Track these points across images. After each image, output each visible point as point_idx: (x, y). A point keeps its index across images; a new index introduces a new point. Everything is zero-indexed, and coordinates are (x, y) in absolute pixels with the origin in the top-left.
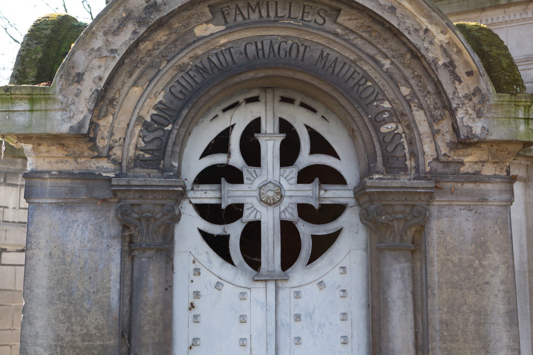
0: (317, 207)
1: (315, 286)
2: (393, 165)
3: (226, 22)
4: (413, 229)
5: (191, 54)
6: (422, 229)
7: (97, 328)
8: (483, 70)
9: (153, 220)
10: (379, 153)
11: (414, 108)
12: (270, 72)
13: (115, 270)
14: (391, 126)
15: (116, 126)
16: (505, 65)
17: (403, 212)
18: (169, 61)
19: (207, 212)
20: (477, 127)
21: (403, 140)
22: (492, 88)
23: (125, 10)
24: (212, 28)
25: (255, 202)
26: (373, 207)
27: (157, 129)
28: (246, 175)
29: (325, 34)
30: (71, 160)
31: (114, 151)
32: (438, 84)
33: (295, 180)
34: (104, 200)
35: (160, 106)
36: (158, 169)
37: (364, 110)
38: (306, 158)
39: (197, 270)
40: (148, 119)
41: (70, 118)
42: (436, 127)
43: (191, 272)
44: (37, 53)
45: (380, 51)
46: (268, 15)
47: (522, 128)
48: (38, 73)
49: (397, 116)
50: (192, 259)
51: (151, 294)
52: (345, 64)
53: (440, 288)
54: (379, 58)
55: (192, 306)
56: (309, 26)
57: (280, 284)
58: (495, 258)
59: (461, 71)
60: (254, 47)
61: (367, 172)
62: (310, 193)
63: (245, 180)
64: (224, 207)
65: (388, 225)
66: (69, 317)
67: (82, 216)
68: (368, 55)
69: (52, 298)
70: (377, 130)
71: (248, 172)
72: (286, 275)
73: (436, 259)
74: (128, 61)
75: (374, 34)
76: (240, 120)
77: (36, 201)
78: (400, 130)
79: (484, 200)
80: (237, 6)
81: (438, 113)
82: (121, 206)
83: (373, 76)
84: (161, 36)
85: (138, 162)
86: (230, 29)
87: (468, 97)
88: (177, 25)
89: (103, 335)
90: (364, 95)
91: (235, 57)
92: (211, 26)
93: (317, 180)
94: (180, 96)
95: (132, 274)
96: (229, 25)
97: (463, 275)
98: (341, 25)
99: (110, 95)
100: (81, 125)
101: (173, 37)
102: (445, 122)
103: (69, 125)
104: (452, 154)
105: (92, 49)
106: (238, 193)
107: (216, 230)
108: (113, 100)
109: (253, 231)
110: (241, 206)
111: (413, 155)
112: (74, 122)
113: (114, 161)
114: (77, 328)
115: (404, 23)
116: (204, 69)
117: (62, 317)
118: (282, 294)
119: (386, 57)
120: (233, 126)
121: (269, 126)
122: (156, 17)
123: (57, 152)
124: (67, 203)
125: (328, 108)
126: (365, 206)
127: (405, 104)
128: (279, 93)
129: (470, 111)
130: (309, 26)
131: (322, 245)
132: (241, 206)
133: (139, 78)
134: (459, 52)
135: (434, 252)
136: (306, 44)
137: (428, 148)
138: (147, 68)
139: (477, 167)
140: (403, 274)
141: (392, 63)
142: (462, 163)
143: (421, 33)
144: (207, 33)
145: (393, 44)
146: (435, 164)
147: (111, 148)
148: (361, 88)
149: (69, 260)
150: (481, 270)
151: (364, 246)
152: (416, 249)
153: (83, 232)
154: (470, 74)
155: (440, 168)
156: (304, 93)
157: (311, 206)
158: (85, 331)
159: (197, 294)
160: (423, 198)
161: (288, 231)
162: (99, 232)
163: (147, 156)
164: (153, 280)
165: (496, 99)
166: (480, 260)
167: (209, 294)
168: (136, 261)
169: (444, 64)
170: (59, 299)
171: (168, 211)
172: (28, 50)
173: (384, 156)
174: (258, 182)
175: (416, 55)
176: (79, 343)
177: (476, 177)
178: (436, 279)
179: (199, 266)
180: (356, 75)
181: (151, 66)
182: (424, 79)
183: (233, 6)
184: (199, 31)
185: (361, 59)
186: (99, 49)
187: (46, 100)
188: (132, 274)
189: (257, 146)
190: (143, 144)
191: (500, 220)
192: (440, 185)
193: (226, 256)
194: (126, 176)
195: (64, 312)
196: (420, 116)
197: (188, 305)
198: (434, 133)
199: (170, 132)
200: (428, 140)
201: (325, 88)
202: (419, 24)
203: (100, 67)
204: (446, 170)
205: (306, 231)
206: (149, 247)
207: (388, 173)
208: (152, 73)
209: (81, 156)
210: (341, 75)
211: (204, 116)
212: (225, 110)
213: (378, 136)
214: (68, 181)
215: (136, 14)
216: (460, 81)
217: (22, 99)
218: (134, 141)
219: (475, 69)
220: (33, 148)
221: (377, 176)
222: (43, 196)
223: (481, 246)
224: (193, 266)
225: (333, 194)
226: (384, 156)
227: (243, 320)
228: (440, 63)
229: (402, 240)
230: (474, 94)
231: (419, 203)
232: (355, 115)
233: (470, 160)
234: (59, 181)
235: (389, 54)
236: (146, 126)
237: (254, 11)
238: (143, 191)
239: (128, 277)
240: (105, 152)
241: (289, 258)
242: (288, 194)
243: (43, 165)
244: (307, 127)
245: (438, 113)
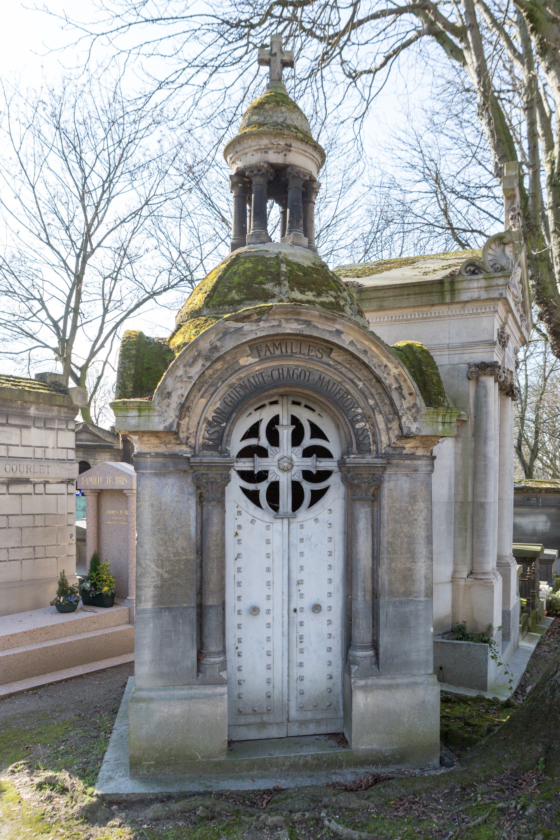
0: (314, 472)
1: (312, 521)
2: (363, 449)
3: (260, 356)
4: (373, 488)
5: (237, 377)
6: (379, 488)
7: (183, 549)
8: (418, 392)
9: (215, 484)
10: (354, 442)
11: (376, 413)
12: (288, 389)
13: (193, 513)
14: (362, 424)
15: (190, 424)
16: (435, 381)
17: (367, 478)
18: (223, 382)
19: (246, 476)
20: (414, 427)
21: (369, 433)
22: (423, 404)
23: (197, 350)
24: (251, 360)
25: (276, 469)
26: (349, 475)
27: (216, 426)
28: (270, 452)
29: (322, 365)
30: (163, 446)
31: (190, 440)
32: (391, 400)
33: (301, 455)
34: (185, 471)
35: (218, 411)
36: (218, 451)
37: (346, 414)
38: (308, 441)
39: (239, 511)
40: (211, 419)
41: (164, 421)
42: (389, 426)
43: (236, 513)
44: (130, 369)
45: (357, 376)
46: (287, 352)
47: (440, 428)
48: (134, 385)
49: (366, 418)
50: (236, 505)
51: (214, 529)
52: (334, 384)
53: (388, 523)
54: (356, 381)
55: (237, 534)
56: (312, 360)
57: (291, 520)
58: (421, 505)
59: (405, 392)
60: (277, 372)
61: (346, 452)
62: (310, 464)
63: (269, 456)
64: (256, 472)
65: (358, 486)
66: (166, 543)
68: (349, 379)
69: (154, 531)
70: (353, 427)
71: (271, 450)
72: (295, 515)
73: (386, 506)
74: (201, 385)
75: (353, 365)
76: (266, 416)
77: (142, 471)
78: (367, 427)
79: (416, 470)
80: (267, 345)
81: (391, 417)
82: (196, 475)
83: (352, 392)
84: (218, 366)
85: (205, 447)
86: (262, 361)
87: (409, 409)
88: (229, 358)
89: (186, 553)
90: (346, 404)
91: (265, 378)
92: (250, 358)
93: (315, 455)
94: (230, 404)
95: (202, 516)
96: (262, 358)
97: (401, 515)
98: (333, 359)
99: (187, 405)
100: (171, 425)
101: (226, 366)
102: (395, 423)
103: (163, 426)
104: (398, 442)
105: (177, 376)
106: (265, 464)
107: (251, 487)
108: (189, 407)
109: (274, 489)
110: (267, 472)
111: (375, 442)
112: (167, 424)
113: (190, 447)
114: (171, 549)
115: (372, 361)
116: (246, 387)
117: (161, 542)
118: (292, 526)
119: (360, 380)
120: (261, 420)
121: (285, 420)
122: (216, 355)
123: (154, 441)
124: (161, 473)
125: (322, 409)
126: (345, 473)
127: (371, 411)
128: (291, 399)
129: (410, 418)
130: (312, 360)
131: (317, 496)
132: (267, 472)
133: (204, 393)
134: (405, 380)
135: (386, 502)
136: (310, 370)
137: (384, 439)
138: (209, 386)
139: (413, 450)
140: (366, 515)
141: (364, 384)
142: (404, 448)
143: (383, 368)
144: (248, 363)
145: (365, 372)
146: (388, 449)
147: (188, 438)
148: (344, 400)
149: (164, 508)
150: (412, 512)
151: (343, 496)
152: (375, 499)
153: (172, 491)
154: (411, 394)
155: (390, 451)
156: (308, 400)
157: (311, 472)
158: (175, 550)
159: (239, 527)
160: (380, 469)
161: (296, 488)
162: (182, 491)
163: (211, 443)
164: (215, 519)
165: (426, 411)
166: (412, 506)
167: (246, 526)
168: (205, 508)
169: (396, 388)
170: (159, 531)
171: (225, 478)
172: (124, 367)
173: (358, 443)
174: (278, 457)
175: (379, 380)
176: (172, 558)
177: (412, 456)
178: (386, 517)
179: (240, 509)
180: (341, 391)
181: (212, 385)
182: (383, 395)
183: (264, 345)
184: (243, 361)
185: (345, 381)
186: (181, 376)
187: (149, 410)
188: (202, 516)
189: (276, 433)
190: (208, 435)
191: (425, 483)
192: (391, 461)
193: (258, 503)
194: (198, 456)
195: (162, 539)
196: (380, 419)
197: (234, 534)
198: (388, 429)
199: (225, 428)
200: (384, 433)
201: (322, 399)
202: (381, 362)
203: (182, 388)
204: (395, 452)
205: (308, 487)
206: (213, 500)
207: (359, 453)
208: (212, 389)
209: (169, 443)
210: (332, 391)
211: (242, 413)
212: (256, 410)
213: (354, 431)
214: (162, 459)
215: (204, 353)
216: (405, 399)
217: (133, 409)
218: (202, 433)
219: (414, 391)
220: (139, 439)
221: (352, 456)
222: (146, 468)
223: (413, 498)
224: (237, 510)
225: (325, 464)
226: (358, 443)
227: (268, 542)
228: (393, 387)
229: (366, 494)
230: (413, 407)
231: (377, 473)
232: (340, 417)
233: (409, 446)
234: (156, 459)
235: (362, 379)
236: (209, 424)
237: (277, 349)
238: (209, 466)
239: (199, 518)
240: (184, 441)
241: (297, 503)
242: (296, 464)
243: (145, 449)
244: (309, 421)
245: (391, 417)
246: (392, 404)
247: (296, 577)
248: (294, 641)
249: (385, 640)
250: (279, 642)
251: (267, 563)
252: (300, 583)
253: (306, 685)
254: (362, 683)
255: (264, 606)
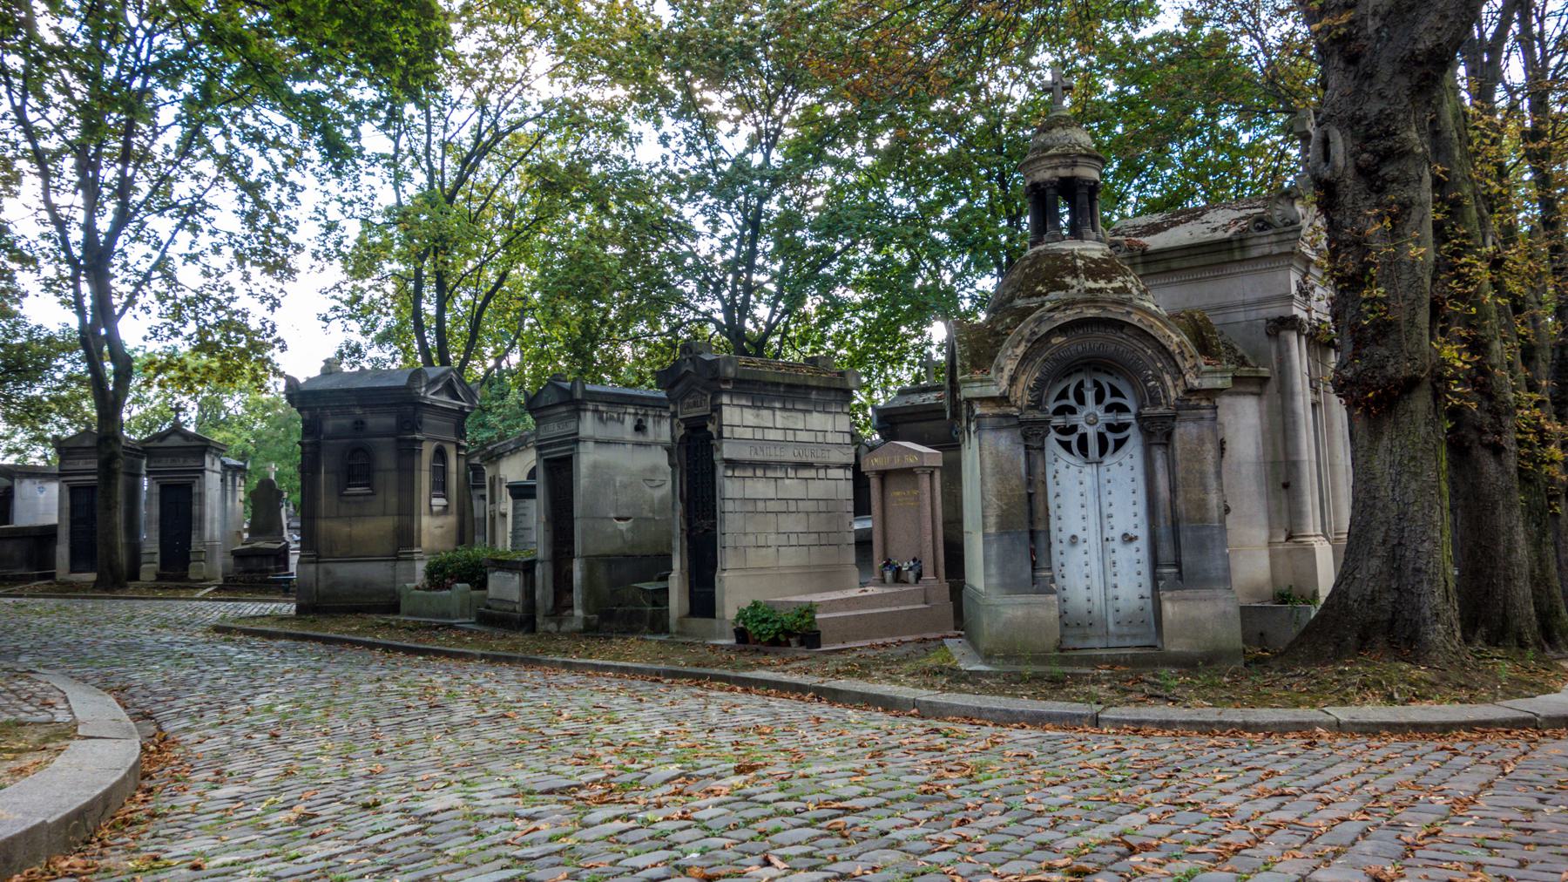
2: (1155, 402)
13: (1023, 458)
51: (1039, 470)
59: (1187, 355)
67: (1004, 434)
85: (1029, 407)
109: (1083, 440)
121: (1088, 384)
124: (997, 429)
131: (1119, 444)
135: (1178, 445)
137: (1173, 394)
161: (1102, 438)
162: (1013, 441)
164: (1039, 463)
167: (1062, 470)
175: (1164, 347)
193: (1070, 450)
196: (1167, 378)
205: (1111, 437)
223: (1201, 441)
241: (1103, 450)
246: (1177, 365)
247: (1106, 511)
248: (1108, 566)
249: (1186, 558)
250: (1095, 567)
251: (1081, 500)
252: (1110, 516)
253: (1120, 604)
254: (1168, 594)
255: (1081, 535)
